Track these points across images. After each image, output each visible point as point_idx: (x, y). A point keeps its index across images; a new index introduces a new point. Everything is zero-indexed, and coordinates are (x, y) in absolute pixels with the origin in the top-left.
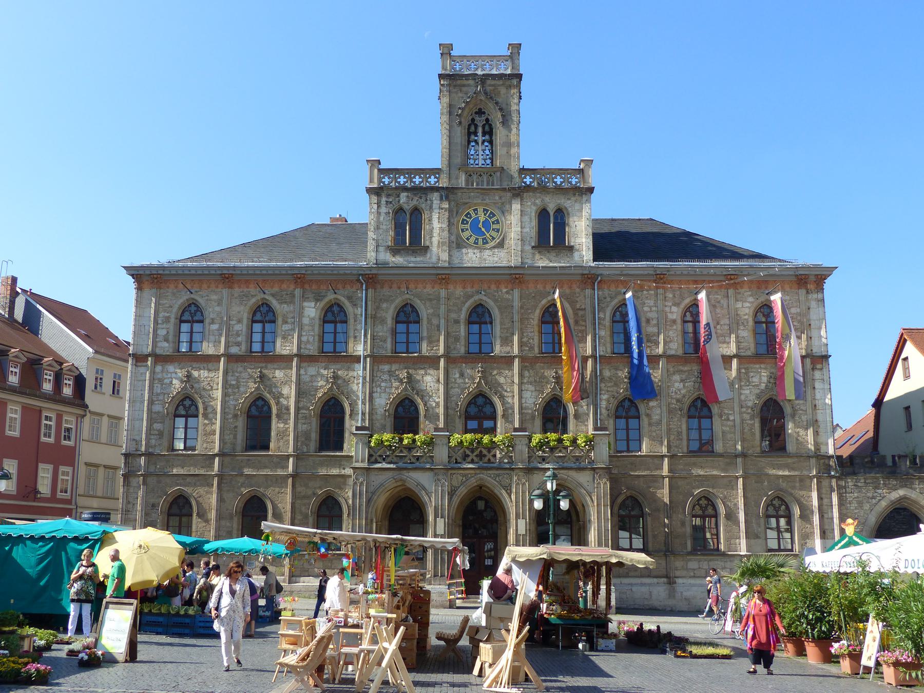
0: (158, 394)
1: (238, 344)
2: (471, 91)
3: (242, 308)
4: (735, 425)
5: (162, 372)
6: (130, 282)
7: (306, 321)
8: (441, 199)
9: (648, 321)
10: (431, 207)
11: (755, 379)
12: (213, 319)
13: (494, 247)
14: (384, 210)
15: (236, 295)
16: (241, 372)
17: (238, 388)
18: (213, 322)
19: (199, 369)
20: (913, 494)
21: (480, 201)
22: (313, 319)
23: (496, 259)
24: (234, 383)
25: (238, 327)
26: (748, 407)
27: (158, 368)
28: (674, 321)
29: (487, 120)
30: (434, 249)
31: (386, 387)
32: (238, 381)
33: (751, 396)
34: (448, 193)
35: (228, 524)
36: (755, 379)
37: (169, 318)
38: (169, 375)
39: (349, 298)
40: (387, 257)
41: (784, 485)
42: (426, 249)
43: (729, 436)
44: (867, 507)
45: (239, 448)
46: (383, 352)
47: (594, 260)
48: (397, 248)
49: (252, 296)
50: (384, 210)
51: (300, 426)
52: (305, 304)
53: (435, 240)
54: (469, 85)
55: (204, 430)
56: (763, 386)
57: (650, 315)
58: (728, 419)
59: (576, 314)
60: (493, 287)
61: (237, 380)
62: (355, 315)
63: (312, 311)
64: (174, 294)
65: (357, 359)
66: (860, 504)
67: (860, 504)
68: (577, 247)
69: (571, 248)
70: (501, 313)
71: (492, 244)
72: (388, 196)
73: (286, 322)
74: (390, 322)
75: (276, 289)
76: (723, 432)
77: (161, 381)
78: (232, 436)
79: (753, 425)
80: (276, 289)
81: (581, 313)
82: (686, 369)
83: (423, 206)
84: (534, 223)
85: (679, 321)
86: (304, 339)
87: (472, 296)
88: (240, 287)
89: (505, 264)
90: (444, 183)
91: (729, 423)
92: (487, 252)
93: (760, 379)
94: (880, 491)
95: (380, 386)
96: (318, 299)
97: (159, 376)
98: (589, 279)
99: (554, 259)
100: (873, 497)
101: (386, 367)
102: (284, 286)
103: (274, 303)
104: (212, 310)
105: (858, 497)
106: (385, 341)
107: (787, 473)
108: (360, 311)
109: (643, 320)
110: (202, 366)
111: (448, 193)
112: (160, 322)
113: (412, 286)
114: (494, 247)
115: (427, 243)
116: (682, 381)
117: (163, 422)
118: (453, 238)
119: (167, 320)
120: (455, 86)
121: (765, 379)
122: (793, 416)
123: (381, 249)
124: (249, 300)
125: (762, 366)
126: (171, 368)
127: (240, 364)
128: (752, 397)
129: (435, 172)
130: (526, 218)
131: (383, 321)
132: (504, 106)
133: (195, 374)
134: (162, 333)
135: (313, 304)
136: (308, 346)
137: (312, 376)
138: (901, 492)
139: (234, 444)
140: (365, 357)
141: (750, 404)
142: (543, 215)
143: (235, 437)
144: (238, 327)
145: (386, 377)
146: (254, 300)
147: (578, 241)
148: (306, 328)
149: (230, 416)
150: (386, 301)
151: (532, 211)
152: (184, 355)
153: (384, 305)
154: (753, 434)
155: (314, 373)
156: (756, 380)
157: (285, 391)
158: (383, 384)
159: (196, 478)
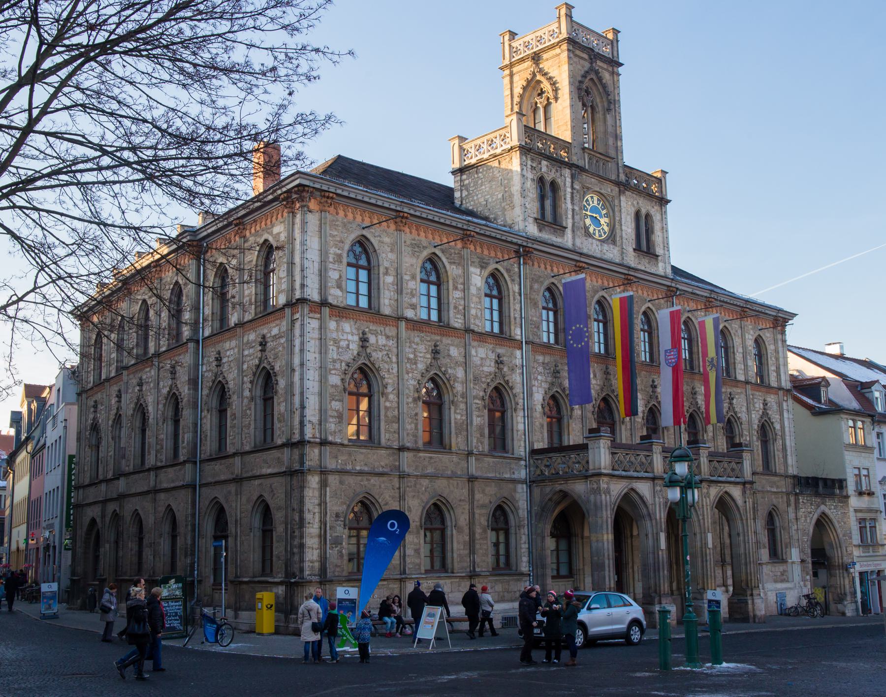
0: (334, 361)
1: (413, 307)
3: (414, 261)
5: (337, 330)
7: (473, 290)
8: (573, 177)
10: (565, 184)
12: (387, 269)
15: (408, 243)
16: (417, 344)
17: (416, 364)
18: (386, 273)
19: (376, 334)
20: (827, 511)
21: (598, 189)
22: (479, 289)
23: (612, 256)
24: (412, 356)
25: (412, 285)
27: (332, 325)
29: (592, 102)
30: (569, 231)
31: (542, 381)
32: (415, 356)
35: (416, 540)
37: (340, 256)
38: (345, 337)
39: (508, 271)
40: (532, 230)
45: (420, 444)
49: (425, 248)
50: (530, 175)
51: (474, 418)
52: (472, 269)
54: (585, 59)
55: (386, 416)
56: (761, 413)
61: (414, 353)
62: (514, 292)
63: (478, 279)
64: (345, 225)
67: (806, 517)
68: (660, 258)
72: (532, 160)
73: (456, 288)
74: (541, 307)
77: (336, 342)
78: (413, 425)
83: (559, 181)
86: (473, 312)
87: (598, 292)
88: (411, 233)
89: (617, 261)
90: (575, 160)
92: (606, 247)
95: (536, 379)
96: (483, 266)
97: (334, 335)
99: (647, 265)
101: (540, 358)
103: (444, 259)
104: (386, 258)
107: (775, 490)
108: (516, 288)
110: (379, 328)
112: (331, 260)
115: (564, 225)
117: (341, 401)
120: (576, 55)
121: (762, 406)
124: (421, 252)
126: (347, 326)
127: (416, 333)
128: (756, 422)
131: (535, 304)
133: (372, 339)
134: (334, 275)
135: (478, 271)
136: (477, 322)
137: (482, 359)
138: (823, 507)
139: (415, 436)
143: (416, 428)
144: (412, 285)
145: (540, 369)
146: (425, 254)
148: (475, 299)
149: (410, 400)
150: (537, 281)
151: (632, 211)
152: (363, 311)
153: (536, 286)
155: (484, 356)
156: (757, 405)
157: (460, 373)
158: (539, 377)
159: (381, 479)
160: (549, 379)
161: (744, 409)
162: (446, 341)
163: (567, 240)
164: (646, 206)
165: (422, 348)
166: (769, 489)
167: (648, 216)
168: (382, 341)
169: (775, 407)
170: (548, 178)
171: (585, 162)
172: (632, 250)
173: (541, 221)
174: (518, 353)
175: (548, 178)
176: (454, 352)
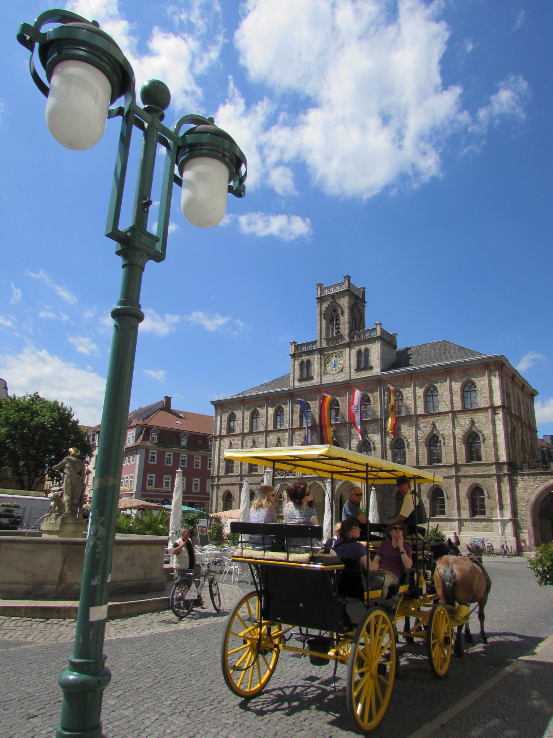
1: (247, 428)
2: (328, 303)
4: (451, 450)
6: (213, 406)
7: (269, 416)
9: (407, 398)
11: (462, 423)
13: (339, 372)
14: (296, 363)
26: (458, 438)
28: (420, 397)
30: (315, 377)
33: (460, 433)
34: (321, 351)
36: (462, 423)
40: (297, 384)
41: (479, 481)
42: (312, 378)
43: (449, 454)
44: (529, 491)
46: (296, 427)
47: (381, 372)
48: (300, 380)
53: (316, 373)
56: (467, 426)
57: (408, 395)
58: (448, 446)
59: (374, 399)
60: (339, 391)
65: (285, 430)
66: (525, 489)
67: (525, 489)
69: (371, 368)
70: (342, 403)
71: (339, 370)
74: (298, 412)
75: (259, 403)
76: (446, 453)
79: (461, 448)
80: (259, 403)
81: (376, 398)
82: (427, 420)
84: (355, 358)
85: (422, 397)
91: (449, 448)
92: (336, 375)
93: (465, 422)
94: (537, 481)
98: (378, 381)
100: (533, 485)
102: (262, 402)
105: (524, 486)
106: (297, 421)
108: (288, 409)
109: (405, 398)
111: (321, 351)
113: (307, 395)
114: (339, 372)
115: (312, 375)
116: (424, 427)
118: (323, 371)
119: (225, 420)
121: (468, 422)
122: (484, 442)
123: (295, 381)
125: (466, 415)
129: (315, 342)
130: (352, 357)
131: (296, 413)
132: (342, 306)
133: (233, 442)
134: (223, 426)
140: (290, 429)
141: (460, 436)
142: (359, 353)
147: (375, 363)
148: (269, 419)
154: (462, 453)
156: (462, 423)
160: (301, 440)
161: (447, 428)
162: (257, 436)
163: (316, 381)
164: (362, 348)
165: (249, 441)
166: (472, 473)
167: (367, 350)
168: (236, 442)
169: (484, 420)
170: (305, 360)
171: (324, 345)
172: (353, 370)
173: (300, 380)
174: (287, 434)
175: (305, 360)
176: (260, 439)
